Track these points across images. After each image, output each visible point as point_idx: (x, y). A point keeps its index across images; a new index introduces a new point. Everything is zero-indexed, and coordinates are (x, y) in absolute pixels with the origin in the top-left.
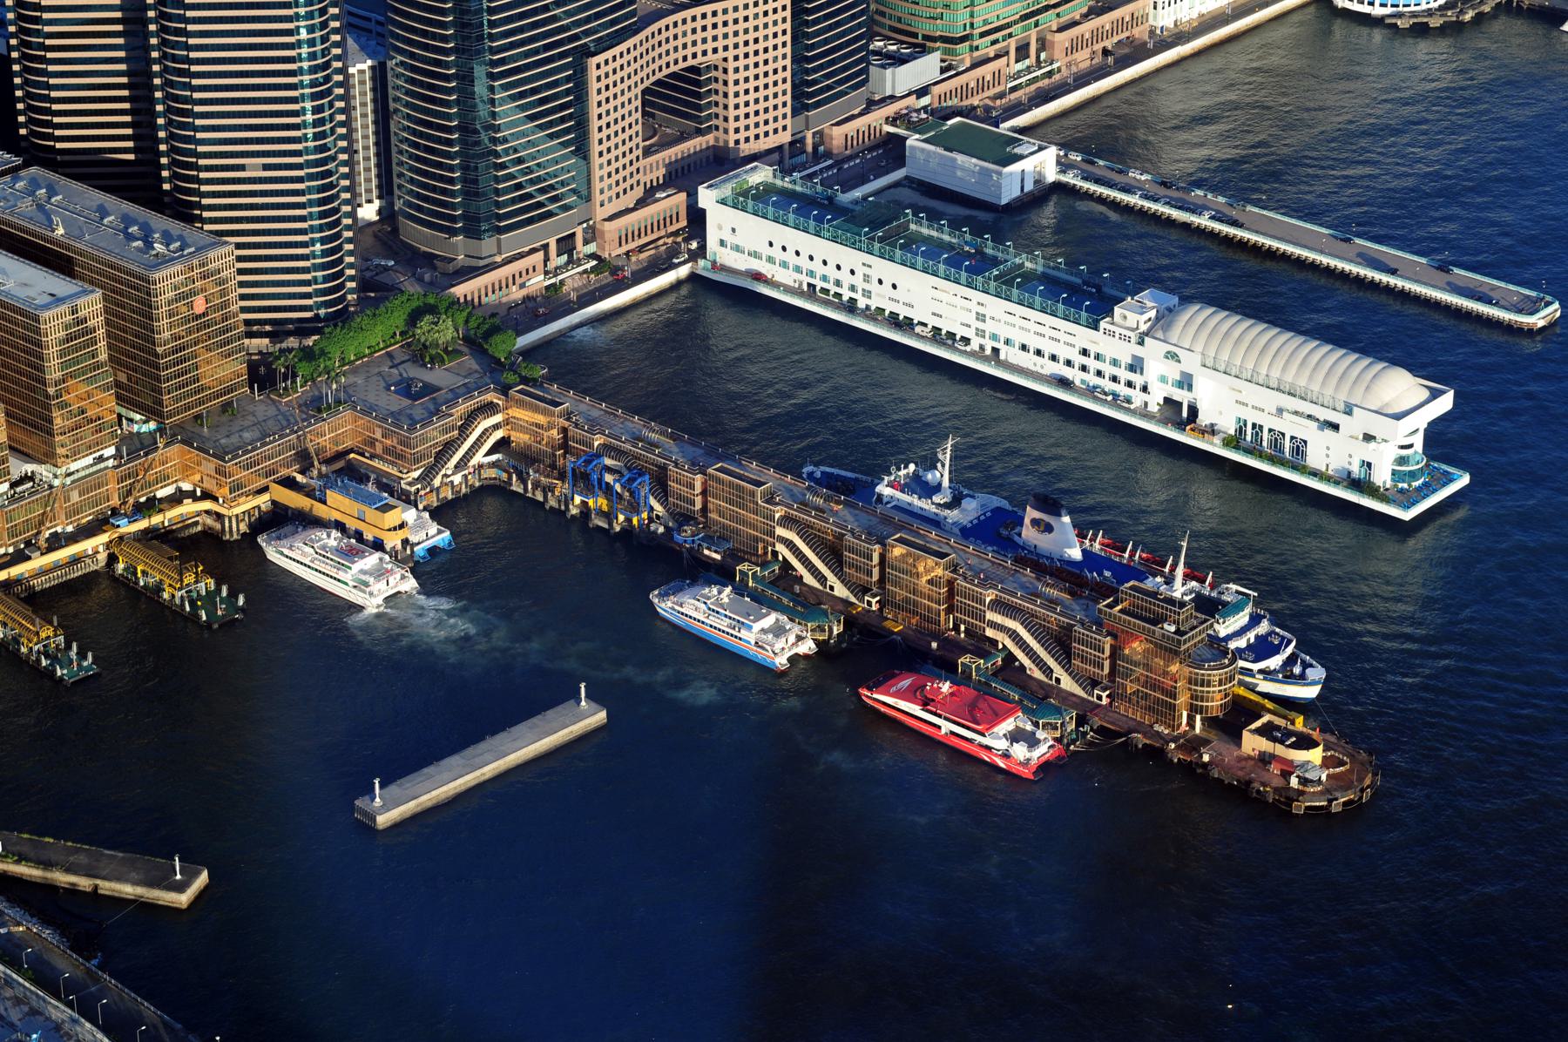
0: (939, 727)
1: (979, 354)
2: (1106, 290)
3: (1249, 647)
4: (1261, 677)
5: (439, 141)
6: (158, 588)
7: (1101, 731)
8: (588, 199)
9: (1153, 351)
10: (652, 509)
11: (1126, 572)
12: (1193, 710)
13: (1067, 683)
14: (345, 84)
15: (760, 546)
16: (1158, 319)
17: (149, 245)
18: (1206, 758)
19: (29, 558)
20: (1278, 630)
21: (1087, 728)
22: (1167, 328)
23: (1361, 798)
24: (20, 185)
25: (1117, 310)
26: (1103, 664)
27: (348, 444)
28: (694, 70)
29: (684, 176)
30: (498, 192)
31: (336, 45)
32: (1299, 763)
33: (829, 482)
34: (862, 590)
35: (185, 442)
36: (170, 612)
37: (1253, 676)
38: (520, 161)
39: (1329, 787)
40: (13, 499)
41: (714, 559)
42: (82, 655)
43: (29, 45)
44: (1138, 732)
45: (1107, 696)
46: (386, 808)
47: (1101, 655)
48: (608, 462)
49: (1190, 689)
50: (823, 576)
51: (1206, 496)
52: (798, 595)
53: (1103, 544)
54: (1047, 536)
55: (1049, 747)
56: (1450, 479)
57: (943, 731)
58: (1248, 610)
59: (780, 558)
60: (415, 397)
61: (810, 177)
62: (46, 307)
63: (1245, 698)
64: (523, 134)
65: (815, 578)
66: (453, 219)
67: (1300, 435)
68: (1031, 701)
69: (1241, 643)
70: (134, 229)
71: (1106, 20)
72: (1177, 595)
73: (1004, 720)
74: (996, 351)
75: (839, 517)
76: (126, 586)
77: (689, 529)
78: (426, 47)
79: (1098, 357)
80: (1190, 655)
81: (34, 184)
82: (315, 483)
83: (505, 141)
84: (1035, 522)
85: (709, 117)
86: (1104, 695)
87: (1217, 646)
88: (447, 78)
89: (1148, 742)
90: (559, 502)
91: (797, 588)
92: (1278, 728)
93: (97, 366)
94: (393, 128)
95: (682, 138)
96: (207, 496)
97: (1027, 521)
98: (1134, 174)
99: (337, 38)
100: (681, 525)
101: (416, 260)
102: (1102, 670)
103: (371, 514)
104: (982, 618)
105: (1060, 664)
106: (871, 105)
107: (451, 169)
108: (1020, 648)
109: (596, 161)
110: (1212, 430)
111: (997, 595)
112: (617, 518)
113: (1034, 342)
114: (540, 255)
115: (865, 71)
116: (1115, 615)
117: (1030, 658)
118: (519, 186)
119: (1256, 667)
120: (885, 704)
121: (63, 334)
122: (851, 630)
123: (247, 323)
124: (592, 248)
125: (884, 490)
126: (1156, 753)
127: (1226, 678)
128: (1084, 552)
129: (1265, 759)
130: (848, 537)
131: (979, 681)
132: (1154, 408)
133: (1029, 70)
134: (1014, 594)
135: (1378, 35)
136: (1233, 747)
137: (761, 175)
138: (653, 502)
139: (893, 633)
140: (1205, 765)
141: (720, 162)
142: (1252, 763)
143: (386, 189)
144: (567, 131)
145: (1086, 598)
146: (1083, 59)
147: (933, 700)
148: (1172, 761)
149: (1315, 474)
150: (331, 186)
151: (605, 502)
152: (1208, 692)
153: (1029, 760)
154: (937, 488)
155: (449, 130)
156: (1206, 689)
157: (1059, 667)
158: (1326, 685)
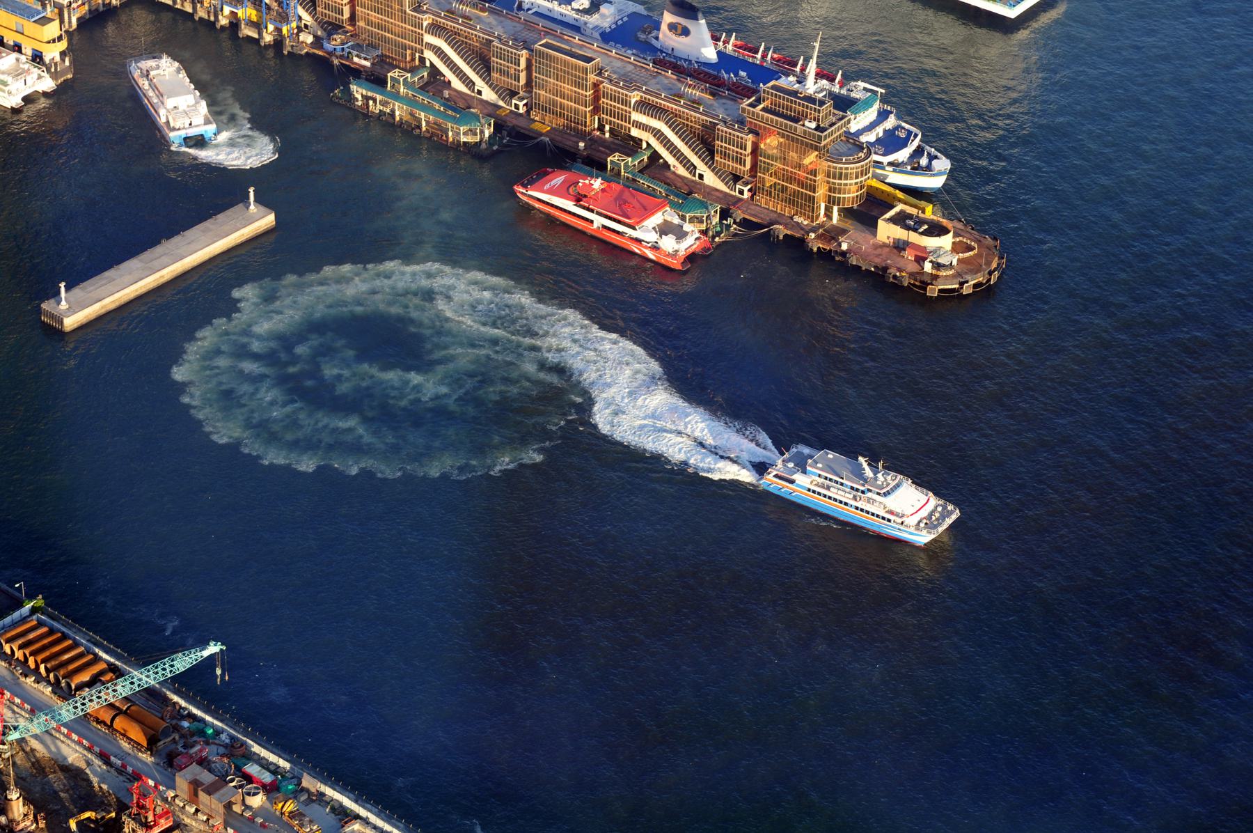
0: (592, 222)
3: (878, 140)
4: (891, 169)
7: (745, 223)
10: (300, 18)
11: (762, 74)
12: (831, 201)
13: (711, 180)
15: (409, 52)
18: (844, 247)
20: (904, 124)
21: (730, 221)
23: (989, 280)
26: (745, 160)
32: (931, 249)
37: (883, 169)
39: (959, 271)
41: (363, 67)
44: (780, 224)
45: (750, 190)
46: (72, 310)
47: (743, 152)
49: (828, 182)
50: (471, 81)
52: (447, 100)
53: (735, 46)
54: (683, 39)
55: (696, 239)
57: (595, 225)
58: (877, 106)
59: (428, 64)
63: (877, 189)
65: (463, 83)
68: (677, 196)
69: (870, 137)
73: (652, 214)
77: (338, 38)
80: (828, 151)
84: (672, 27)
86: (746, 189)
87: (853, 142)
89: (789, 232)
90: (209, 13)
91: (446, 93)
92: (910, 217)
97: (664, 27)
100: (329, 35)
102: (744, 166)
103: (30, 27)
104: (627, 119)
105: (703, 160)
108: (664, 146)
111: (641, 97)
112: (266, 28)
116: (758, 114)
117: (674, 156)
119: (885, 160)
120: (539, 200)
122: (500, 133)
126: (796, 244)
127: (862, 171)
128: (719, 53)
129: (900, 246)
130: (496, 43)
131: (628, 178)
134: (658, 96)
136: (869, 236)
138: (301, 12)
139: (542, 134)
140: (844, 254)
142: (888, 249)
145: (725, 97)
147: (585, 196)
148: (812, 250)
151: (254, 12)
152: (846, 185)
153: (677, 251)
156: (843, 182)
157: (702, 164)
158: (951, 174)
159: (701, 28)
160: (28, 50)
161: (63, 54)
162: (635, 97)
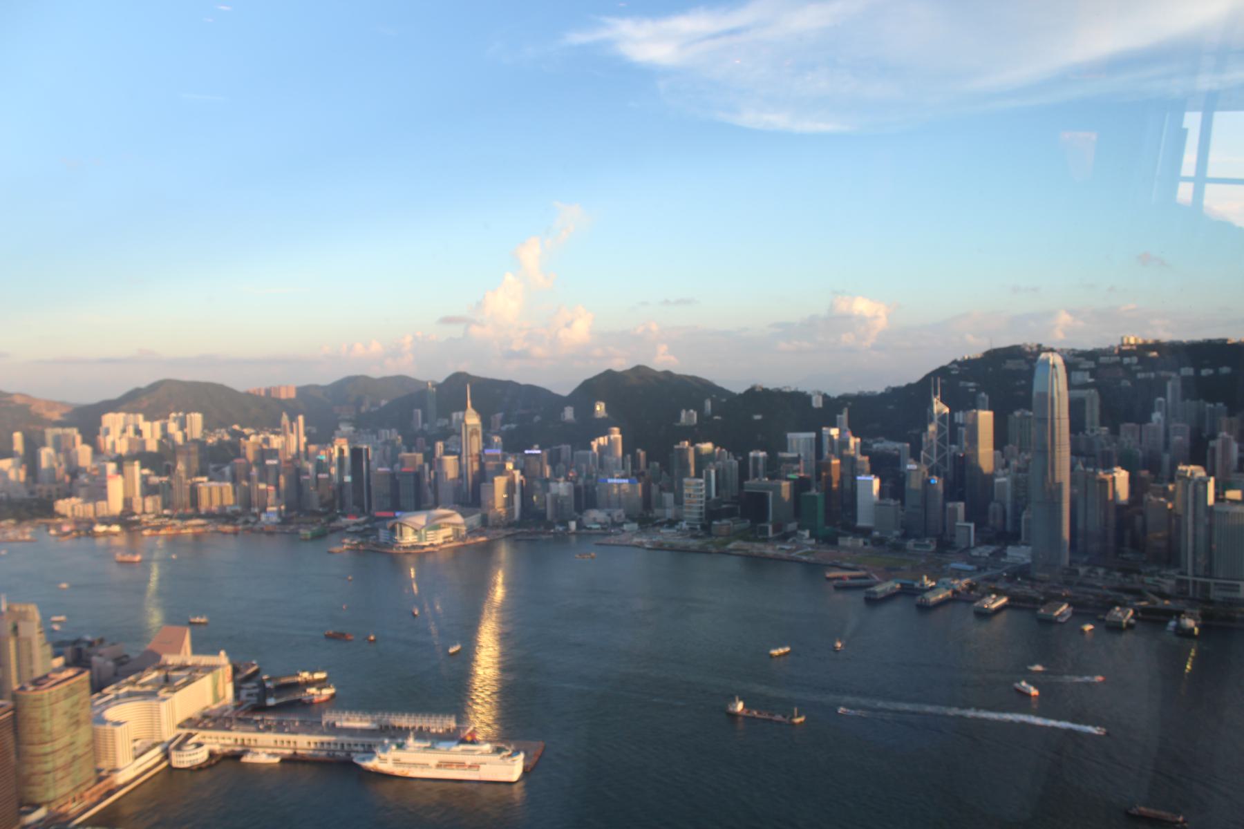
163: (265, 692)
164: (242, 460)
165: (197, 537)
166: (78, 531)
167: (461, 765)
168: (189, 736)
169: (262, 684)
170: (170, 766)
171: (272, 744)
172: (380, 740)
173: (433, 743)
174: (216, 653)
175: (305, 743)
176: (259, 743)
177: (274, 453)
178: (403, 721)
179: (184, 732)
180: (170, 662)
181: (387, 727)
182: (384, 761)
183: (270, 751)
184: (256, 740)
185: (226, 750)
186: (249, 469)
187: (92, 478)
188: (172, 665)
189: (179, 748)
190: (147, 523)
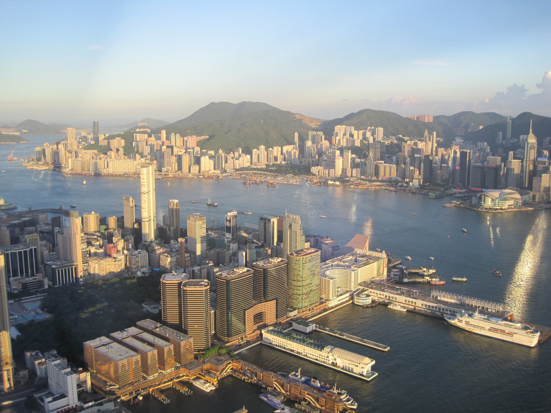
1: (304, 355)
2: (323, 345)
5: (223, 323)
6: (180, 390)
8: (245, 331)
9: (330, 354)
11: (327, 389)
12: (337, 410)
13: (318, 406)
14: (210, 314)
16: (331, 350)
17: (180, 338)
19: (160, 385)
22: (332, 351)
24: (162, 328)
25: (325, 349)
27: (209, 368)
28: (261, 312)
29: (260, 328)
30: (232, 330)
31: (209, 308)
33: (282, 375)
34: (287, 391)
35: (185, 368)
36: (182, 394)
38: (235, 326)
40: (159, 376)
42: (168, 400)
43: (164, 308)
48: (248, 371)
51: (338, 377)
56: (375, 374)
58: (345, 394)
60: (220, 361)
61: (278, 329)
62: (165, 347)
64: (236, 322)
66: (225, 334)
67: (352, 367)
69: (345, 399)
70: (178, 335)
71: (322, 305)
72: (335, 392)
74: (306, 355)
75: (283, 380)
76: (175, 389)
77: (260, 382)
78: (222, 309)
79: (322, 356)
81: (164, 328)
82: (204, 374)
83: (233, 323)
84: (313, 381)
85: (263, 320)
87: (341, 400)
88: (225, 313)
93: (172, 356)
94: (217, 321)
95: (260, 322)
96: (187, 376)
98: (326, 328)
99: (209, 307)
101: (220, 340)
103: (212, 379)
106: (287, 318)
107: (225, 327)
109: (246, 326)
110: (339, 367)
113: (312, 353)
114: (238, 340)
115: (286, 313)
118: (235, 330)
121: (167, 351)
123: (195, 350)
124: (246, 339)
125: (290, 376)
128: (320, 386)
132: (330, 363)
133: (311, 313)
135: (361, 308)
137: (271, 328)
141: (265, 326)
143: (215, 330)
144: (242, 321)
146: (318, 311)
149: (354, 373)
150: (207, 329)
154: (298, 376)
155: (225, 321)
158: (358, 406)
159: (318, 381)
160: (211, 383)
161: (217, 384)
162: (306, 392)
163: (402, 275)
164: (402, 153)
165: (376, 191)
166: (320, 183)
167: (503, 332)
168: (363, 291)
169: (401, 270)
170: (353, 303)
171: (404, 302)
172: (460, 310)
173: (488, 317)
174: (381, 252)
175: (420, 304)
176: (397, 301)
177: (419, 151)
178: (474, 302)
179: (362, 288)
180: (358, 252)
181: (464, 304)
182: (461, 321)
183: (402, 305)
184: (396, 298)
185: (381, 300)
186: (405, 159)
187: (329, 157)
188: (359, 254)
189: (358, 295)
190: (353, 182)
